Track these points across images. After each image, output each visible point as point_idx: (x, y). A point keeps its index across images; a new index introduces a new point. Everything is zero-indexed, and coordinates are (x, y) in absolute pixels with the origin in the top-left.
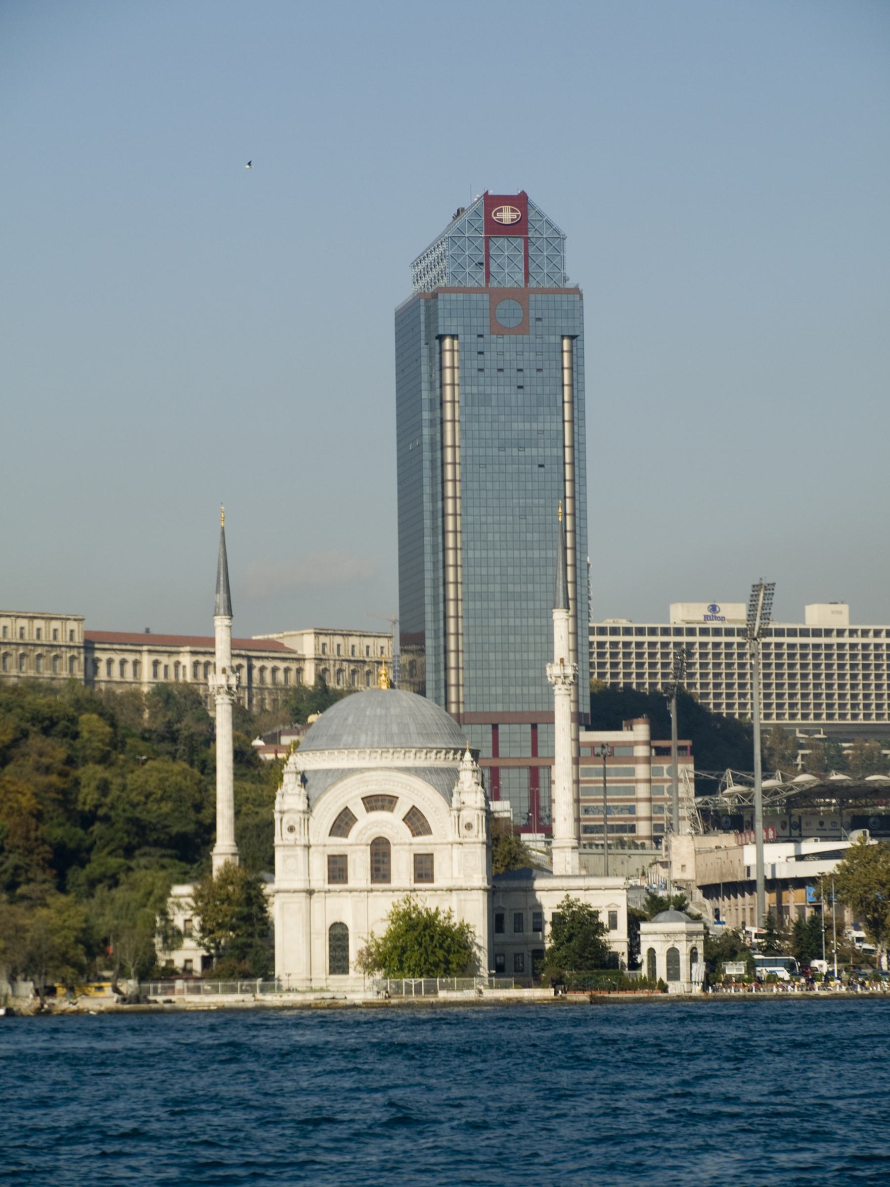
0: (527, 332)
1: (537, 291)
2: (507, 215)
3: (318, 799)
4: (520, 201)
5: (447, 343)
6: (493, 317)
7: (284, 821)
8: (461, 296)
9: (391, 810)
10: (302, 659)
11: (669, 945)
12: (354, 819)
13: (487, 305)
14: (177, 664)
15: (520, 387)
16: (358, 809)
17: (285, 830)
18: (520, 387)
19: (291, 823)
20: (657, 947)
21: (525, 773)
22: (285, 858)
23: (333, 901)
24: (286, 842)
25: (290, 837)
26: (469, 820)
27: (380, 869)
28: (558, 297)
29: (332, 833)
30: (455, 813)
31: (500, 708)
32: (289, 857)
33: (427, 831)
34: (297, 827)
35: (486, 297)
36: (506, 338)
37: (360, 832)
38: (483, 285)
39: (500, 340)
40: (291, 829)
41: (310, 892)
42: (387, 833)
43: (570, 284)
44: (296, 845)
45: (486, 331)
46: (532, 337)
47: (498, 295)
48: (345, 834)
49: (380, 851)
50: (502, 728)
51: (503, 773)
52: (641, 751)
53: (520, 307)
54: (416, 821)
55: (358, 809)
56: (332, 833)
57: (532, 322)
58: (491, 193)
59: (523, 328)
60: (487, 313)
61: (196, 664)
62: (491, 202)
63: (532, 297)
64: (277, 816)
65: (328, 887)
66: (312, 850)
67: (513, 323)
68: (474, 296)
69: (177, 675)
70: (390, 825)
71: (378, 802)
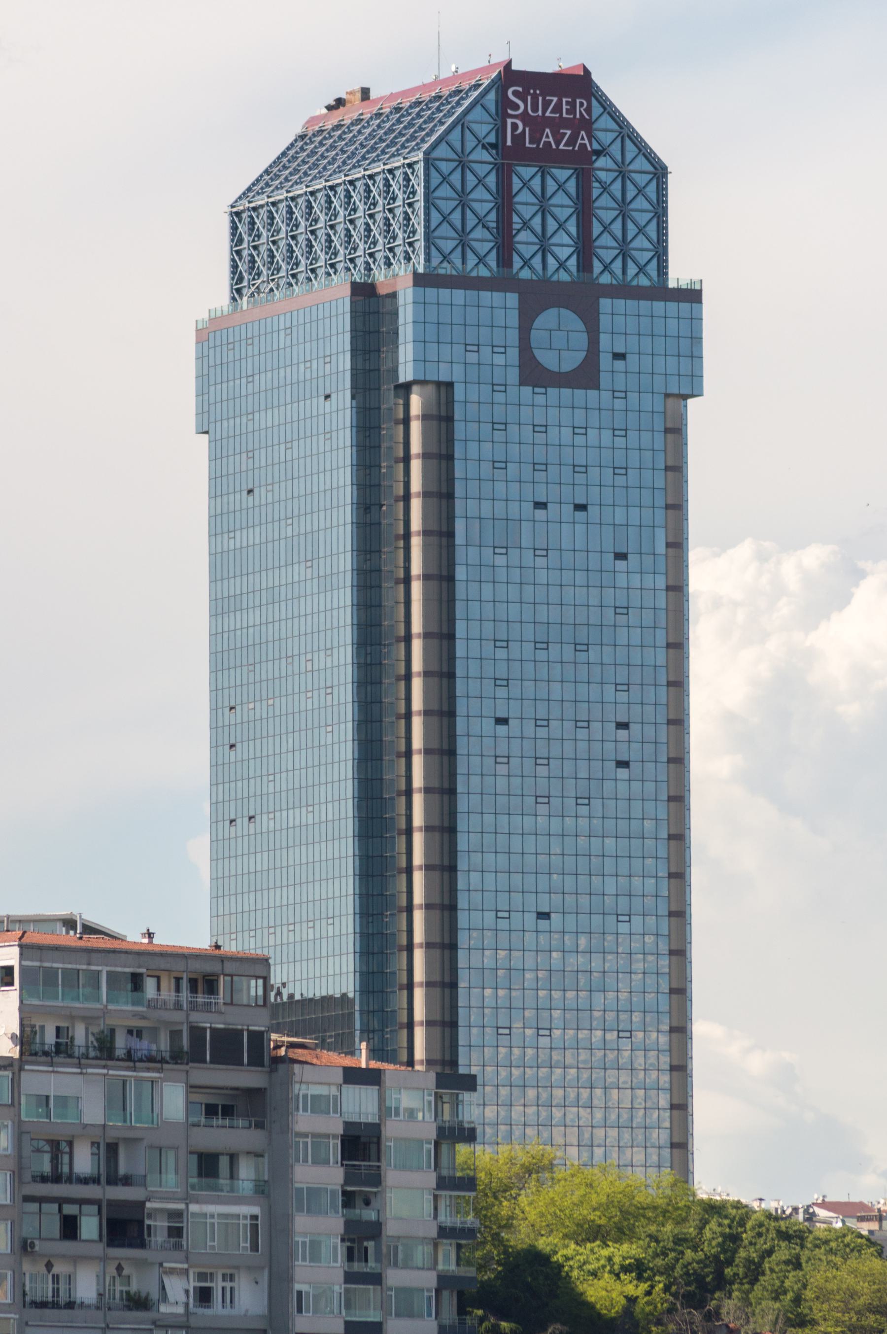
0: (595, 384)
6: (525, 347)
8: (459, 295)
13: (513, 318)
15: (581, 508)
18: (581, 508)
28: (659, 306)
35: (512, 299)
39: (540, 399)
45: (513, 375)
46: (606, 395)
53: (579, 325)
57: (605, 361)
58: (515, 67)
59: (586, 376)
60: (513, 336)
63: (605, 304)
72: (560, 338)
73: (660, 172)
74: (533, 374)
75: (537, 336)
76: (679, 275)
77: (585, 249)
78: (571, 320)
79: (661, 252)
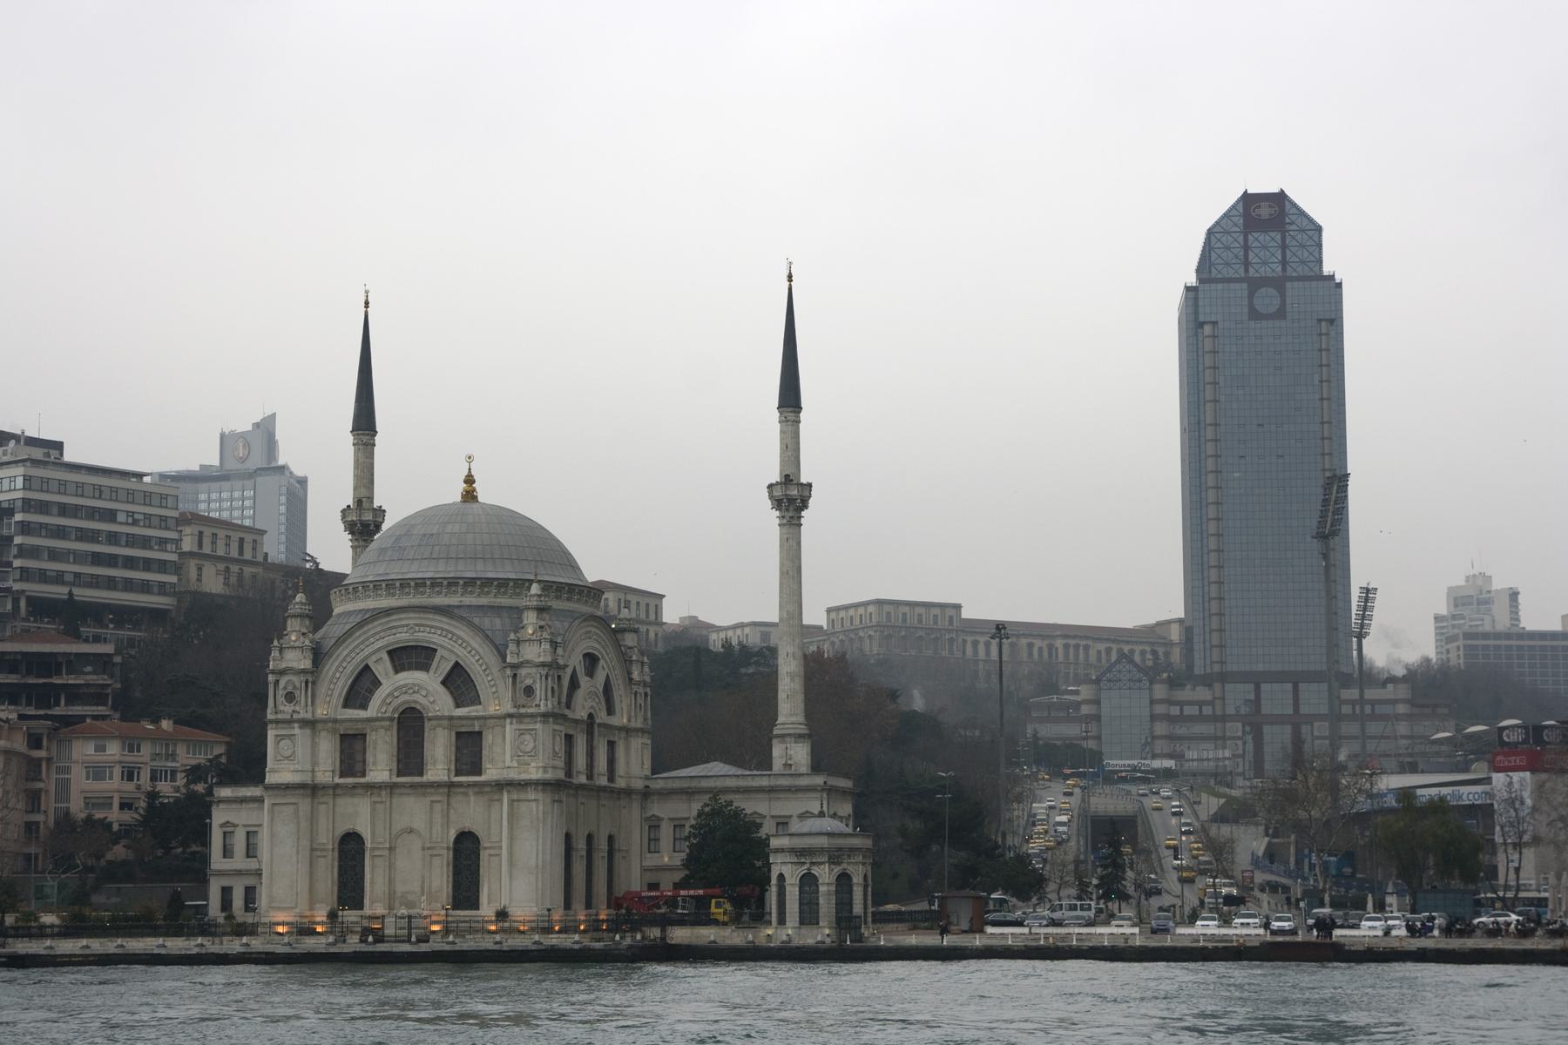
1: (1292, 279)
2: (1265, 211)
3: (329, 654)
4: (1280, 198)
5: (1207, 329)
7: (282, 684)
8: (1220, 286)
9: (425, 667)
10: (1171, 644)
11: (803, 870)
12: (377, 683)
14: (1050, 647)
16: (383, 668)
17: (280, 699)
19: (290, 689)
20: (786, 870)
21: (1288, 729)
22: (279, 738)
23: (346, 804)
24: (280, 716)
25: (287, 709)
26: (529, 682)
27: (410, 757)
28: (1314, 284)
29: (347, 703)
30: (508, 672)
31: (1261, 667)
32: (283, 737)
33: (476, 700)
34: (297, 693)
35: (1245, 286)
36: (1264, 323)
37: (384, 701)
38: (1242, 273)
40: (290, 697)
41: (312, 790)
42: (420, 700)
43: (1327, 270)
44: (290, 722)
45: (1246, 317)
47: (1255, 284)
48: (364, 707)
49: (410, 724)
50: (1264, 687)
51: (1267, 729)
52: (1402, 709)
54: (459, 682)
55: (383, 668)
56: (347, 703)
59: (1280, 314)
60: (1246, 302)
61: (1066, 646)
62: (1248, 199)
63: (1288, 285)
64: (271, 678)
65: (338, 780)
66: (319, 726)
67: (1273, 309)
68: (1233, 286)
69: (1050, 655)
70: (427, 689)
71: (410, 656)
72: (1267, 300)
73: (1319, 229)
74: (1254, 315)
75: (1257, 302)
76: (1327, 270)
77: (1284, 263)
78: (1272, 291)
79: (1320, 262)
